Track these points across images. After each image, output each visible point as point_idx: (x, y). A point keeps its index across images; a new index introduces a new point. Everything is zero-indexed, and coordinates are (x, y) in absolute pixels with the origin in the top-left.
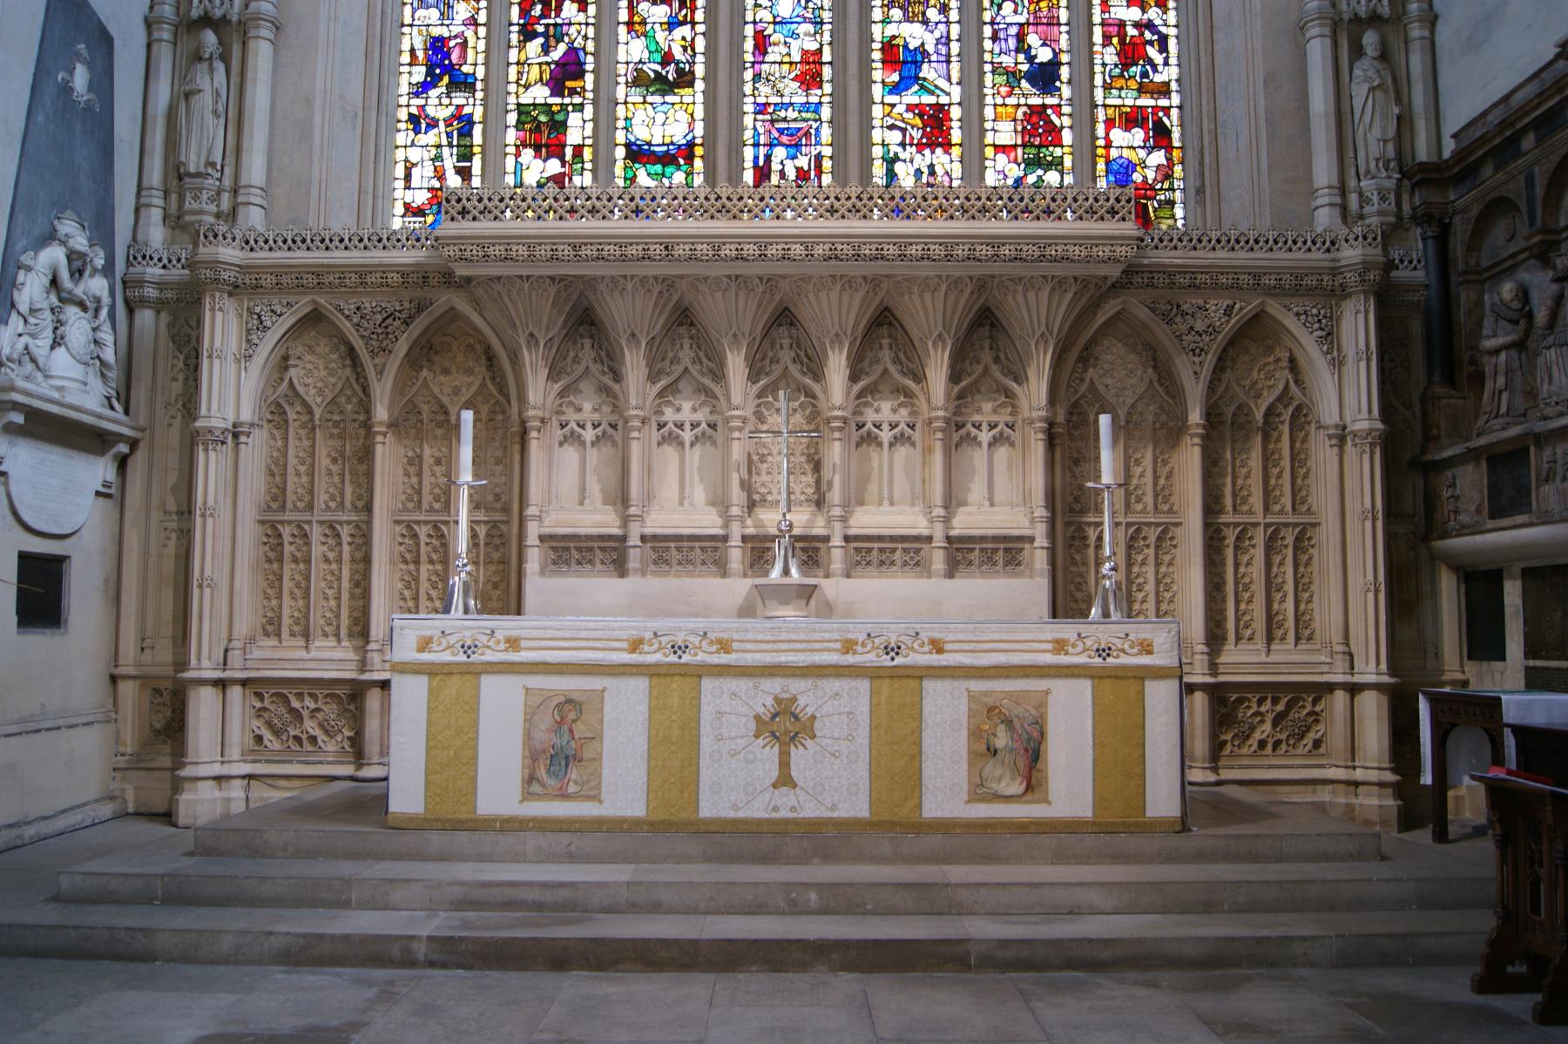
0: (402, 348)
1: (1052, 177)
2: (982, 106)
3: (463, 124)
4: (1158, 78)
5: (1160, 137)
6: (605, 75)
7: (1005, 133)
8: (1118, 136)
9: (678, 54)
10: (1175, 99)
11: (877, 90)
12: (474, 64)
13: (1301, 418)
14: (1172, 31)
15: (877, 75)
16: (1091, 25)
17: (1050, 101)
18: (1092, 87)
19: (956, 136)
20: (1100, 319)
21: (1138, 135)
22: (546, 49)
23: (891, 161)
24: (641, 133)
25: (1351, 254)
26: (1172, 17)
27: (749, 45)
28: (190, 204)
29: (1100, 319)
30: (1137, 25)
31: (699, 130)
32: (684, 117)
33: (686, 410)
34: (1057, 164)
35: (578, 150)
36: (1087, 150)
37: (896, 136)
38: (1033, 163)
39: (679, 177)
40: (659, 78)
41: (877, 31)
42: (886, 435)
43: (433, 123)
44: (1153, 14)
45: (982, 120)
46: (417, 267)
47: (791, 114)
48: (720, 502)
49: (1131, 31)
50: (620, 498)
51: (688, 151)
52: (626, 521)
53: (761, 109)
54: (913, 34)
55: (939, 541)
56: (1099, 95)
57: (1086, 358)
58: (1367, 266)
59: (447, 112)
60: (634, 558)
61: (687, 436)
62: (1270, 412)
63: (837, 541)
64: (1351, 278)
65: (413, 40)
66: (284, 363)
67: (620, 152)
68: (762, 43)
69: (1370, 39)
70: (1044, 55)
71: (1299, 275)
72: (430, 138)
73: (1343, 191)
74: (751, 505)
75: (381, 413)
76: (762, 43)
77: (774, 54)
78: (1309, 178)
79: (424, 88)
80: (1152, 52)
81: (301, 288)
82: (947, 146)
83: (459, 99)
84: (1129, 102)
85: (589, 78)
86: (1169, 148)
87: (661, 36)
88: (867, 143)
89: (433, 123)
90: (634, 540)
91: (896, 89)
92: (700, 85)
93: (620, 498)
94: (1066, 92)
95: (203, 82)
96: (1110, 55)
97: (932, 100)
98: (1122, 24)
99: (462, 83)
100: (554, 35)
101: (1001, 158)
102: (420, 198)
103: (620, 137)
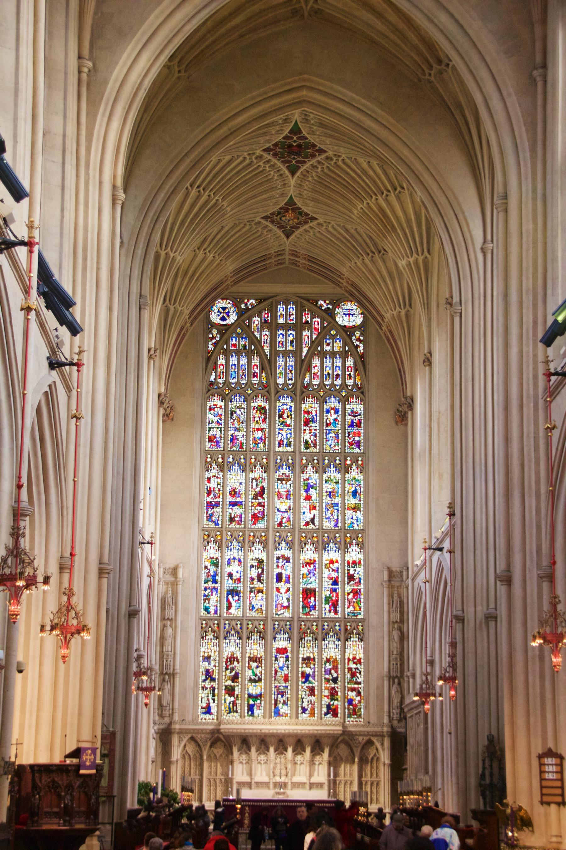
0: (209, 744)
1: (336, 703)
2: (321, 686)
3: (213, 689)
4: (359, 680)
5: (359, 694)
6: (243, 678)
7: (326, 693)
8: (350, 693)
9: (259, 674)
10: (362, 685)
11: (300, 683)
12: (215, 675)
13: (378, 759)
14: (362, 670)
15: (300, 679)
16: (345, 668)
17: (336, 685)
18: (345, 682)
19: (316, 693)
20: (339, 740)
21: (354, 693)
22: (231, 672)
23: (302, 699)
24: (251, 691)
25: (385, 729)
26: (362, 666)
27: (274, 672)
28: (164, 712)
29: (339, 740)
30: (355, 669)
31: (263, 691)
32: (259, 688)
33: (262, 757)
34: (337, 700)
35: (237, 695)
36: (345, 697)
37: (304, 693)
38: (332, 700)
39: (259, 701)
40: (255, 679)
41: (300, 669)
42: (299, 762)
43: (207, 689)
44: (359, 666)
45: (322, 689)
46: (213, 730)
47: (282, 688)
48: (268, 775)
49: (354, 670)
50: (250, 774)
51: (260, 695)
52: (251, 779)
53: (276, 687)
54: (308, 671)
55: (308, 783)
56: (346, 684)
57: (337, 747)
58: (388, 732)
59: (210, 686)
60: (253, 786)
61: (262, 762)
62: (372, 758)
63: (290, 783)
64: (385, 734)
65: (202, 670)
66: (185, 746)
67: (246, 696)
68: (276, 672)
69: (396, 681)
70: (335, 675)
71: (376, 732)
72: (206, 692)
73: (389, 712)
74: (274, 776)
75: (205, 757)
76: (276, 672)
77: (279, 674)
78: (383, 709)
79: (204, 681)
80: (358, 675)
81: (189, 733)
82: (314, 695)
83: (212, 683)
84: (353, 686)
85: (240, 679)
86: (361, 696)
87: (255, 670)
88: (297, 694)
89: (207, 689)
90: (253, 783)
91: (304, 683)
92: (263, 681)
93: (250, 774)
94: (339, 683)
95: (166, 687)
96: (348, 676)
97: (311, 685)
98: (351, 669)
99: (213, 680)
100: (233, 669)
101: (326, 698)
102: (204, 705)
103: (246, 692)
